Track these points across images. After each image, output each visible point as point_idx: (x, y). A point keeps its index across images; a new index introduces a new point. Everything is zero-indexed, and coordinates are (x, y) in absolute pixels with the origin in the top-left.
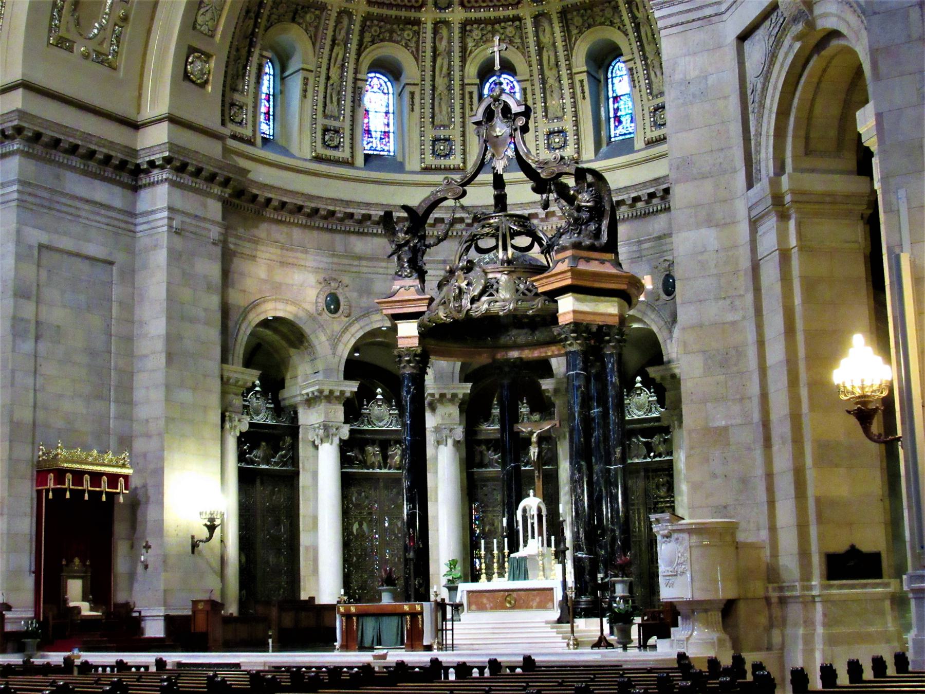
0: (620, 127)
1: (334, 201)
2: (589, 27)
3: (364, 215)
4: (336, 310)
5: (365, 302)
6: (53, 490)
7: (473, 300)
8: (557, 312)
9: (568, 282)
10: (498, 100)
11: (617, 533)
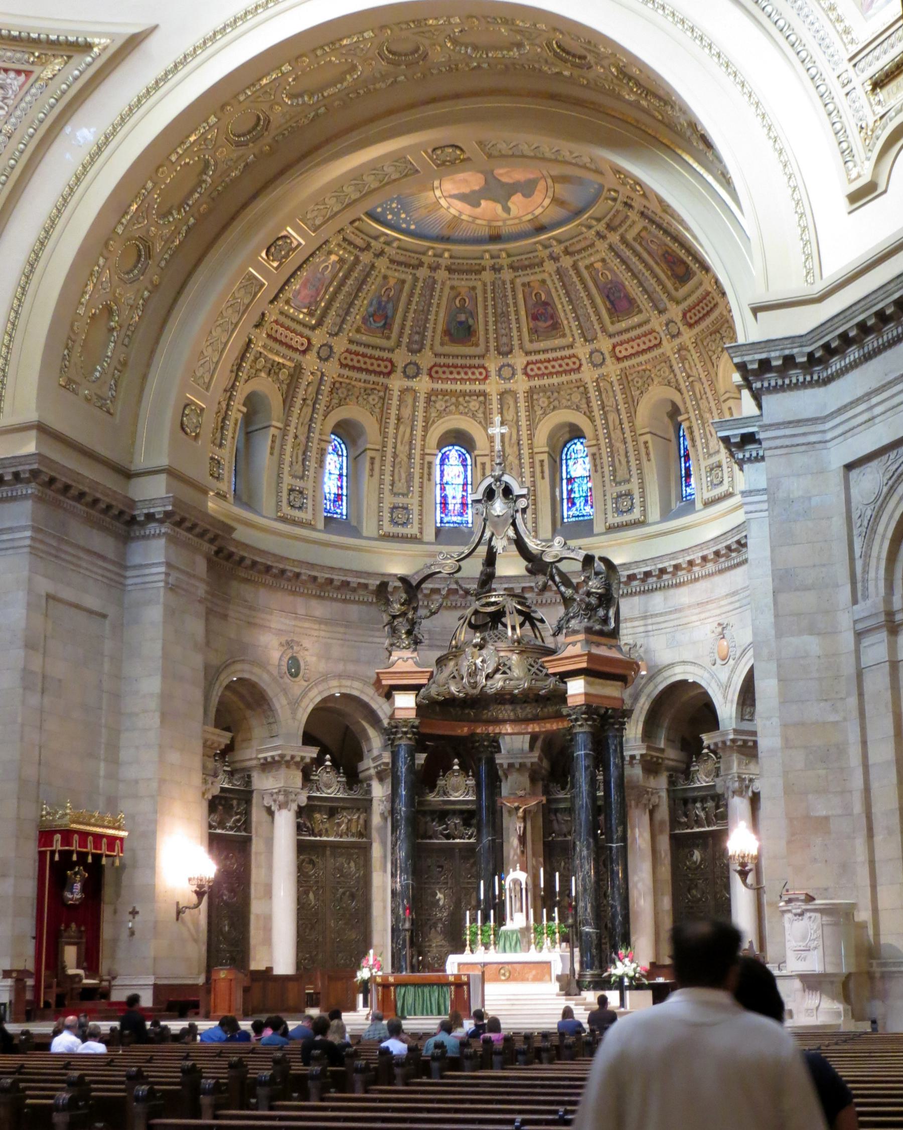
0: (574, 509)
1: (301, 563)
2: (554, 408)
3: (327, 579)
4: (296, 675)
6: (60, 852)
7: (488, 677)
8: (566, 693)
9: (584, 665)
10: (500, 481)
11: (619, 909)
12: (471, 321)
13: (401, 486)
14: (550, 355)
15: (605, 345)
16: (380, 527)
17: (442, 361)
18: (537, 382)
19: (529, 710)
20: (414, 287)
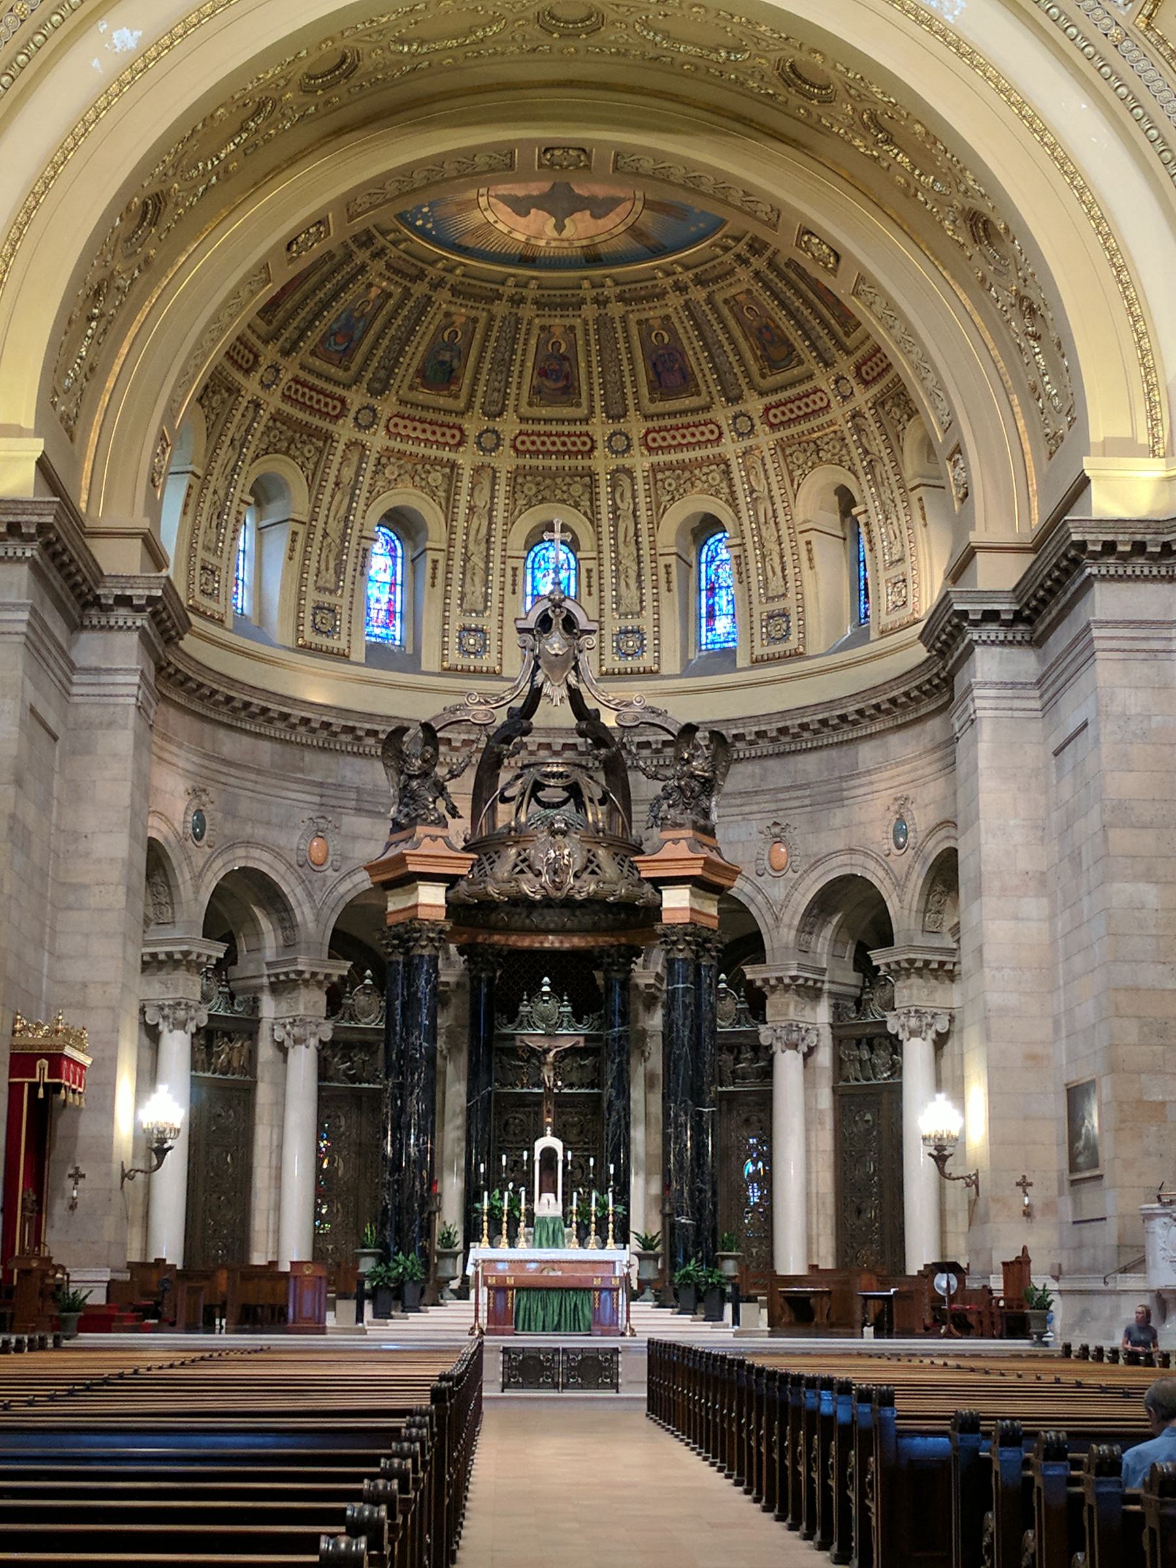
5: (229, 828)
8: (661, 905)
9: (698, 872)
12: (455, 363)
13: (329, 577)
14: (554, 428)
15: (636, 427)
16: (299, 634)
17: (407, 411)
19: (552, 918)
20: (400, 305)
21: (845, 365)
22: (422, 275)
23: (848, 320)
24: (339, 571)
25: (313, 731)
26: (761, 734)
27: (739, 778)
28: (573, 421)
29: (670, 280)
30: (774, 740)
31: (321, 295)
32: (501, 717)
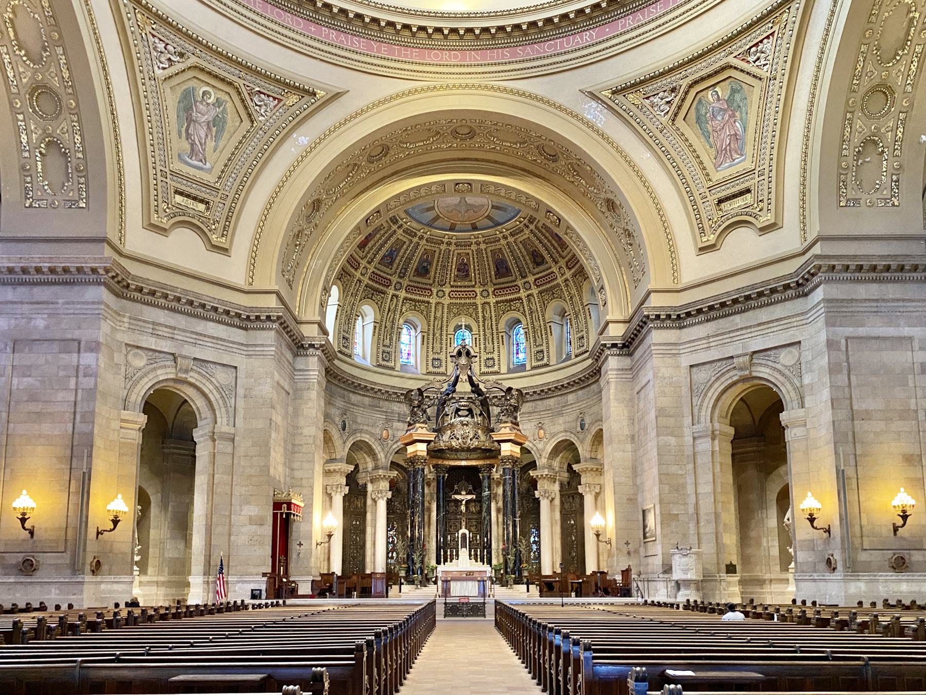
12: (429, 267)
13: (387, 342)
16: (378, 361)
18: (454, 301)
21: (562, 263)
22: (415, 235)
23: (563, 245)
24: (391, 339)
25: (383, 394)
26: (534, 392)
27: (526, 407)
28: (469, 287)
29: (502, 235)
30: (539, 394)
31: (380, 242)
32: (446, 386)
